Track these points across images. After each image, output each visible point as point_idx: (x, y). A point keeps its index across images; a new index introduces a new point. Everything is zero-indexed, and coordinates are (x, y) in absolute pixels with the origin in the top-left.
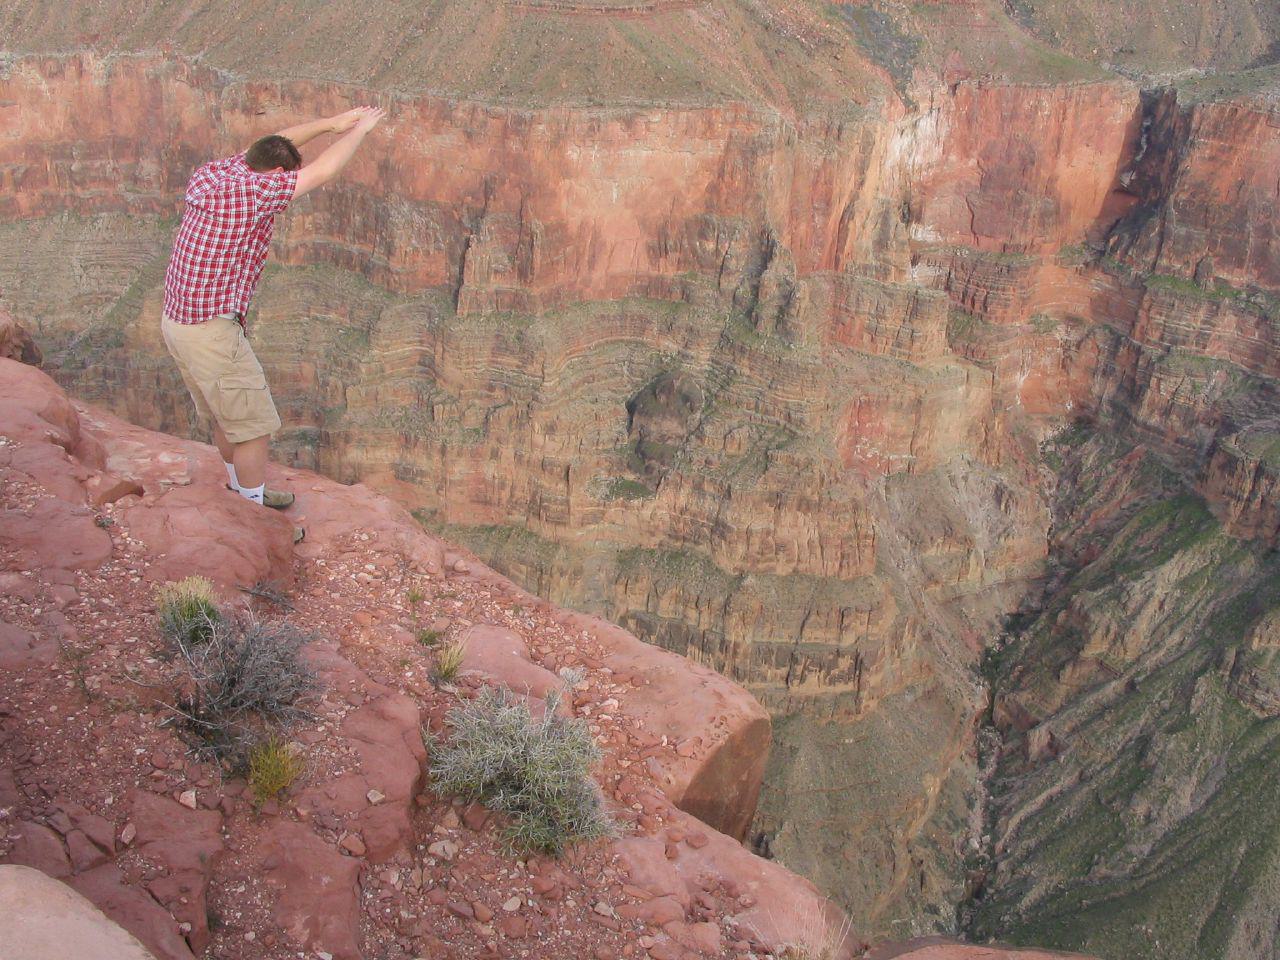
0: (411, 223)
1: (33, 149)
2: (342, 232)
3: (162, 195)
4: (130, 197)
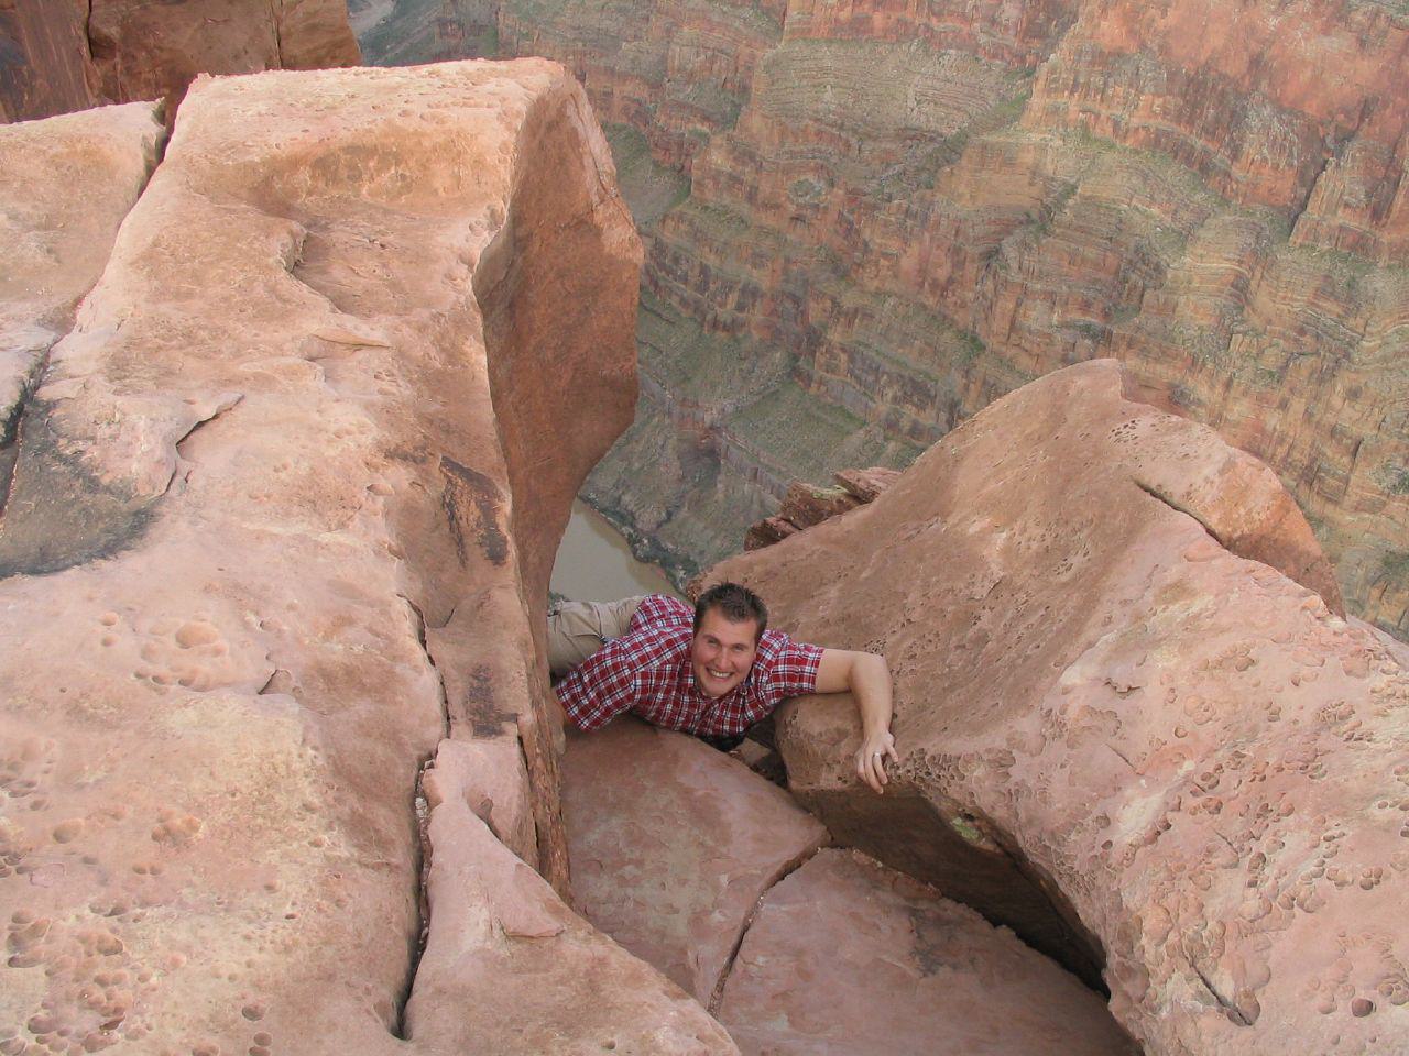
0: (1267, 128)
2: (1190, 122)
3: (1015, 44)
4: (983, 39)
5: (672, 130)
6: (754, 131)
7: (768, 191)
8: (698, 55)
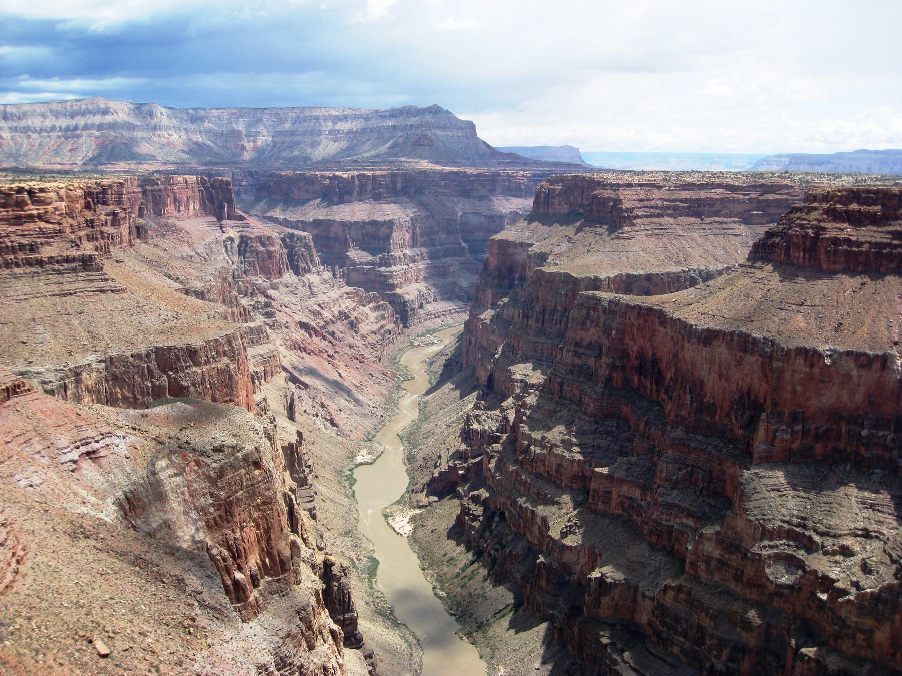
1: (835, 414)
5: (664, 523)
6: (738, 529)
7: (752, 574)
8: (680, 469)
